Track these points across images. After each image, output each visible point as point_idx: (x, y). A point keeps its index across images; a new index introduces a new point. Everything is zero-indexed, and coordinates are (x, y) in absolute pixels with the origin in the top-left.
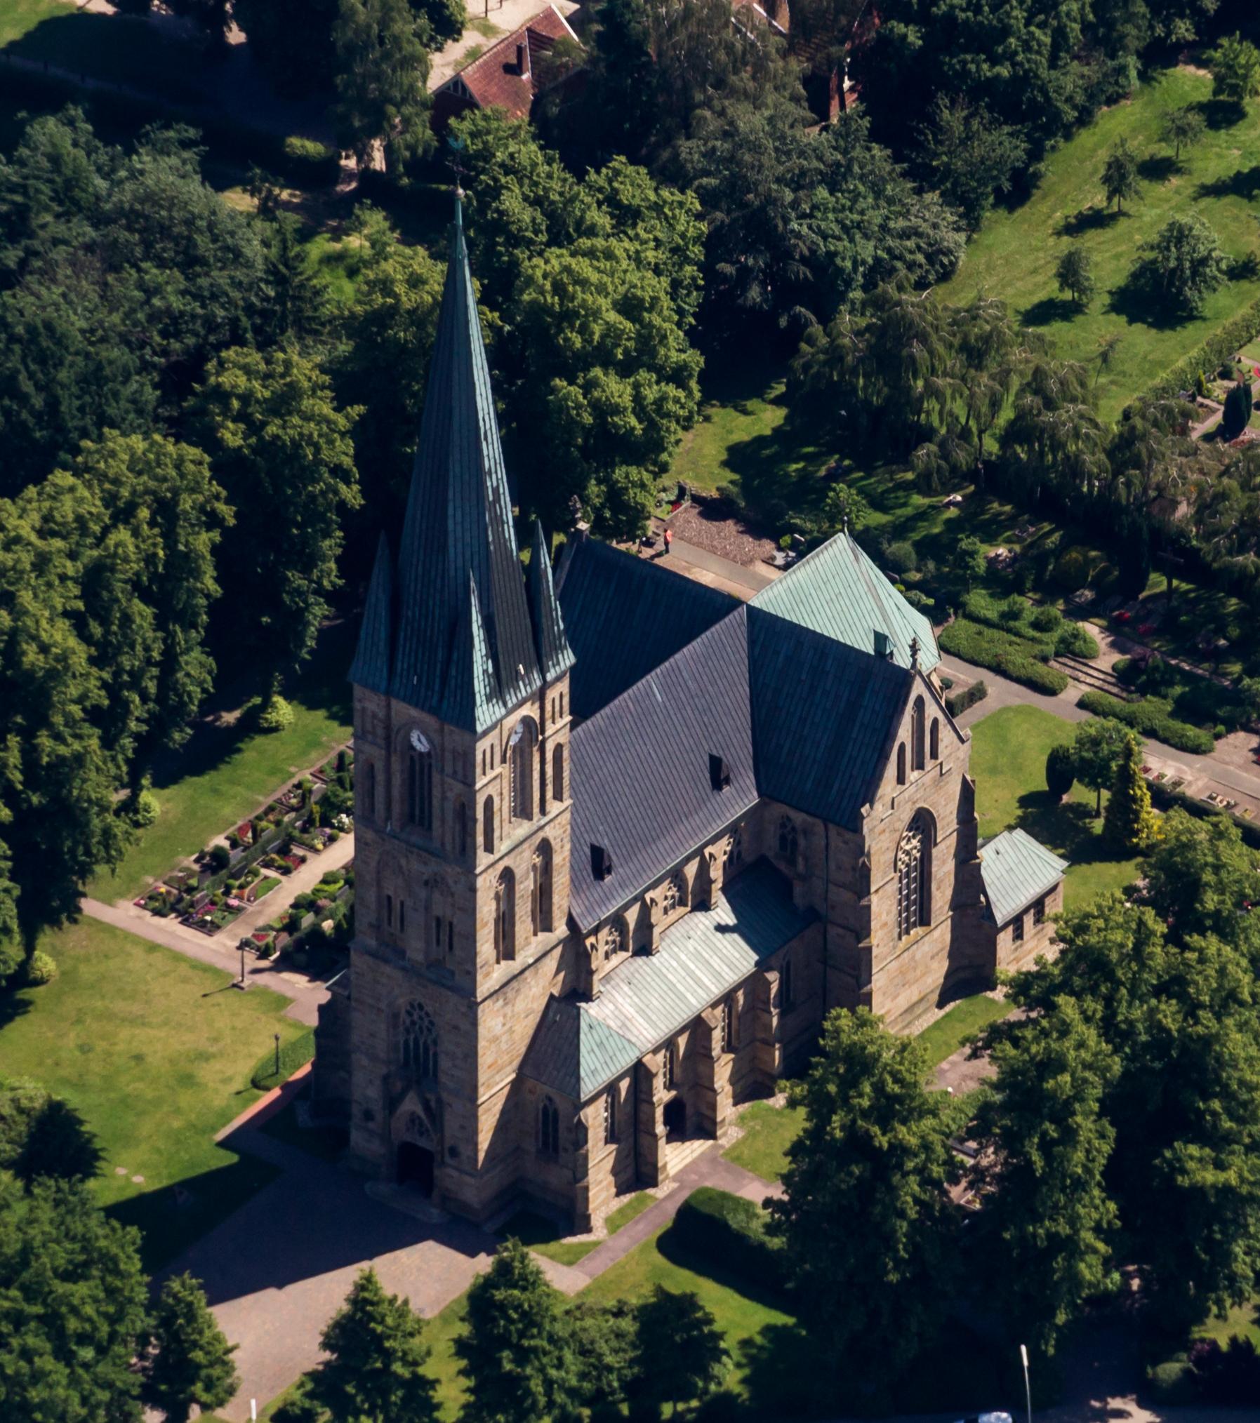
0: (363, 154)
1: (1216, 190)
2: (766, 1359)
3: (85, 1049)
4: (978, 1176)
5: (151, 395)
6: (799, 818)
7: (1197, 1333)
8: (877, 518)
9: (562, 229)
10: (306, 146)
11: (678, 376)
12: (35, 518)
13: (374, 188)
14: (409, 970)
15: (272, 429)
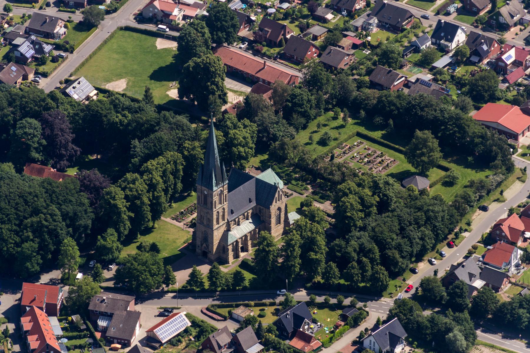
2: (252, 282)
10: (204, 118)
11: (251, 148)
14: (204, 226)
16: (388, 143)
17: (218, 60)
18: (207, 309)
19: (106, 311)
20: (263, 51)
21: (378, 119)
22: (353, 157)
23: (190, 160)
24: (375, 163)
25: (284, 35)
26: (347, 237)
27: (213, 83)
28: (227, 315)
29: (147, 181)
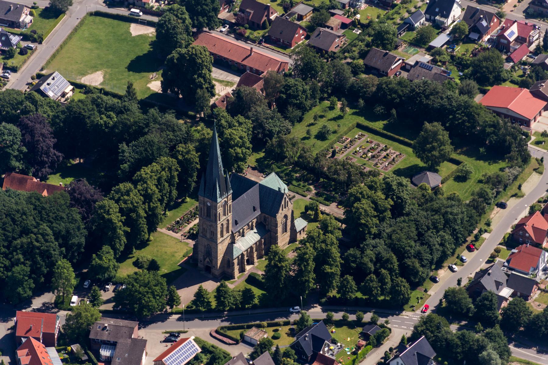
0: (200, 114)
1: (331, 120)
2: (262, 299)
3: (158, 251)
4: (294, 270)
5: (168, 151)
6: (267, 216)
7: (328, 294)
8: (279, 170)
9: (230, 126)
11: (248, 148)
12: (150, 170)
13: (202, 119)
14: (207, 239)
15: (186, 156)
16: (392, 135)
17: (205, 51)
18: (217, 332)
19: (109, 340)
20: (247, 35)
21: (378, 109)
22: (356, 152)
23: (185, 165)
24: (380, 158)
25: (268, 16)
26: (362, 246)
27: (200, 75)
28: (239, 338)
29: (142, 192)
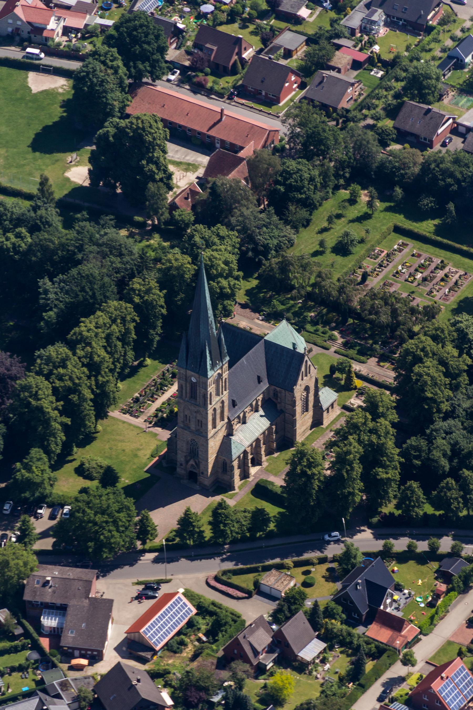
1: (353, 221)
12: (94, 324)
15: (146, 298)
